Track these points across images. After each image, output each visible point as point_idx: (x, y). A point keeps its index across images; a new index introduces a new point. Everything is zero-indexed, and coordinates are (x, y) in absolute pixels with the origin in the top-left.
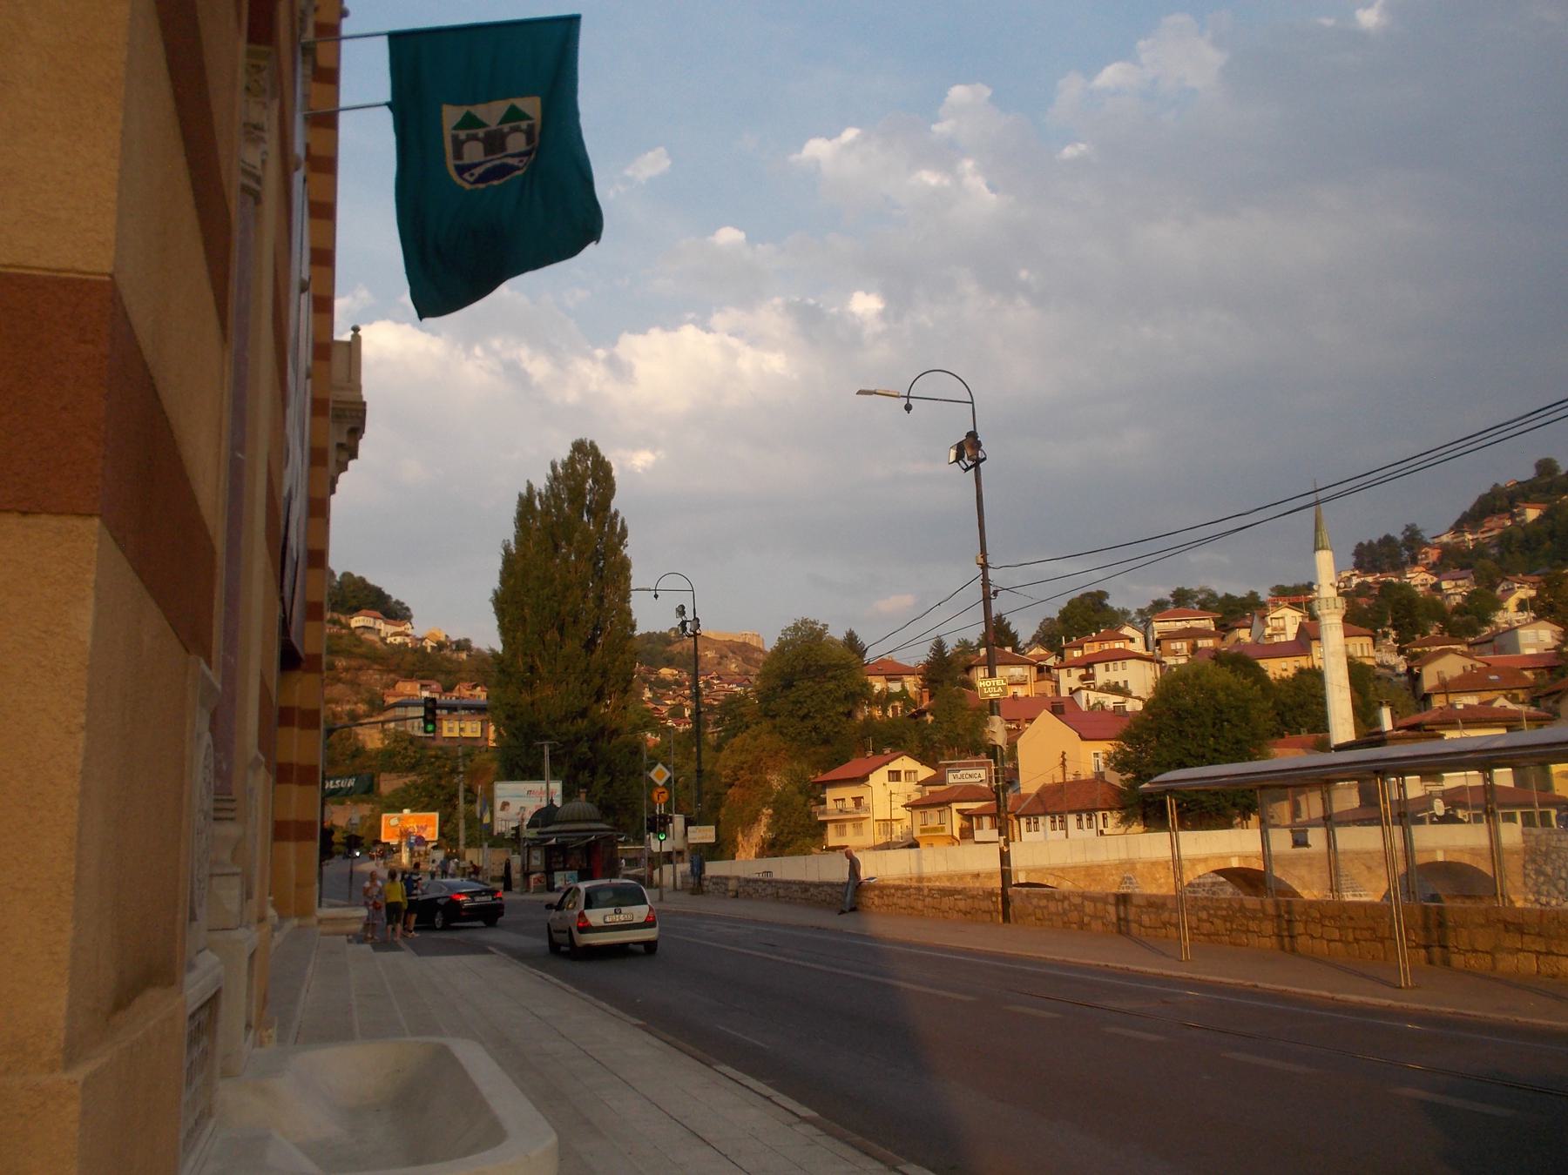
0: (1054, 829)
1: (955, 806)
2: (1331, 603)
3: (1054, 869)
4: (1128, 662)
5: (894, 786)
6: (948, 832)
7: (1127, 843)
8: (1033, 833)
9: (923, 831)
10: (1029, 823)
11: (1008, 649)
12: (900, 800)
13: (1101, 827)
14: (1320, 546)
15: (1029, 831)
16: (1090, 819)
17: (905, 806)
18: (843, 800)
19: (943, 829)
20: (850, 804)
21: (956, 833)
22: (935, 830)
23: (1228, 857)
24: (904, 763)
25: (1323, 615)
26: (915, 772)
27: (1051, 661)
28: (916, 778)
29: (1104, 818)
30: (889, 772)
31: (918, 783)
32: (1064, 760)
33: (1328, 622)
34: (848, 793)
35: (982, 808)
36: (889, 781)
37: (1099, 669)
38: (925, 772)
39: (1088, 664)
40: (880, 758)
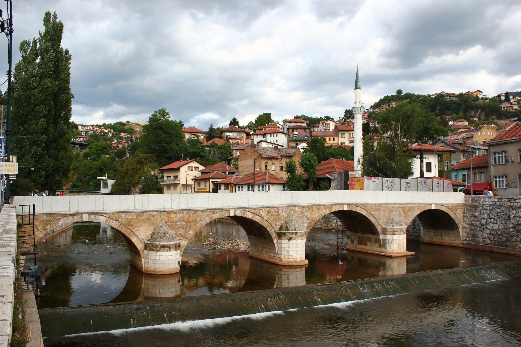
0: (248, 190)
1: (211, 180)
2: (359, 108)
3: (250, 208)
4: (278, 135)
5: (189, 172)
6: (208, 190)
7: (292, 195)
8: (240, 192)
9: (198, 189)
10: (239, 188)
11: (237, 126)
12: (190, 177)
13: (267, 190)
14: (357, 87)
15: (239, 190)
16: (263, 187)
17: (192, 180)
18: (170, 177)
19: (206, 189)
20: (172, 178)
21: (211, 191)
22: (203, 189)
23: (343, 205)
24: (194, 164)
25: (356, 113)
26: (198, 168)
27: (251, 133)
28: (198, 170)
29: (269, 187)
30: (188, 167)
31: (199, 172)
32: (255, 163)
33: (357, 116)
34: (172, 175)
35: (221, 181)
36: (188, 170)
37: (268, 136)
38: (202, 168)
39: (264, 135)
40: (185, 162)
